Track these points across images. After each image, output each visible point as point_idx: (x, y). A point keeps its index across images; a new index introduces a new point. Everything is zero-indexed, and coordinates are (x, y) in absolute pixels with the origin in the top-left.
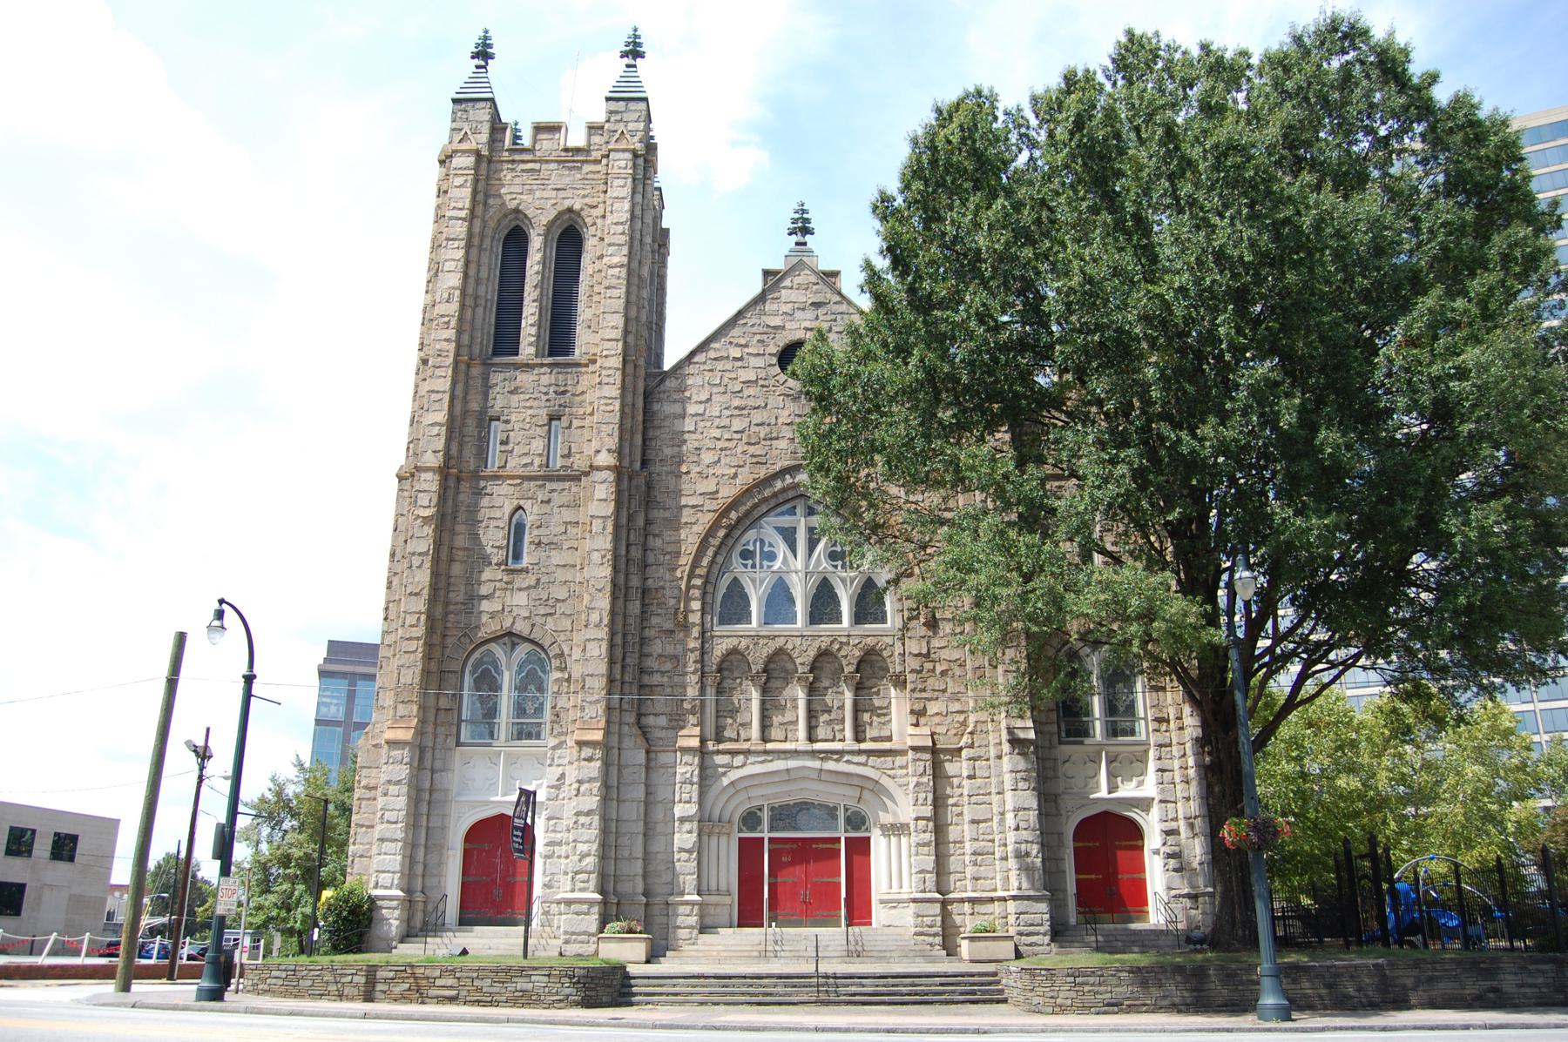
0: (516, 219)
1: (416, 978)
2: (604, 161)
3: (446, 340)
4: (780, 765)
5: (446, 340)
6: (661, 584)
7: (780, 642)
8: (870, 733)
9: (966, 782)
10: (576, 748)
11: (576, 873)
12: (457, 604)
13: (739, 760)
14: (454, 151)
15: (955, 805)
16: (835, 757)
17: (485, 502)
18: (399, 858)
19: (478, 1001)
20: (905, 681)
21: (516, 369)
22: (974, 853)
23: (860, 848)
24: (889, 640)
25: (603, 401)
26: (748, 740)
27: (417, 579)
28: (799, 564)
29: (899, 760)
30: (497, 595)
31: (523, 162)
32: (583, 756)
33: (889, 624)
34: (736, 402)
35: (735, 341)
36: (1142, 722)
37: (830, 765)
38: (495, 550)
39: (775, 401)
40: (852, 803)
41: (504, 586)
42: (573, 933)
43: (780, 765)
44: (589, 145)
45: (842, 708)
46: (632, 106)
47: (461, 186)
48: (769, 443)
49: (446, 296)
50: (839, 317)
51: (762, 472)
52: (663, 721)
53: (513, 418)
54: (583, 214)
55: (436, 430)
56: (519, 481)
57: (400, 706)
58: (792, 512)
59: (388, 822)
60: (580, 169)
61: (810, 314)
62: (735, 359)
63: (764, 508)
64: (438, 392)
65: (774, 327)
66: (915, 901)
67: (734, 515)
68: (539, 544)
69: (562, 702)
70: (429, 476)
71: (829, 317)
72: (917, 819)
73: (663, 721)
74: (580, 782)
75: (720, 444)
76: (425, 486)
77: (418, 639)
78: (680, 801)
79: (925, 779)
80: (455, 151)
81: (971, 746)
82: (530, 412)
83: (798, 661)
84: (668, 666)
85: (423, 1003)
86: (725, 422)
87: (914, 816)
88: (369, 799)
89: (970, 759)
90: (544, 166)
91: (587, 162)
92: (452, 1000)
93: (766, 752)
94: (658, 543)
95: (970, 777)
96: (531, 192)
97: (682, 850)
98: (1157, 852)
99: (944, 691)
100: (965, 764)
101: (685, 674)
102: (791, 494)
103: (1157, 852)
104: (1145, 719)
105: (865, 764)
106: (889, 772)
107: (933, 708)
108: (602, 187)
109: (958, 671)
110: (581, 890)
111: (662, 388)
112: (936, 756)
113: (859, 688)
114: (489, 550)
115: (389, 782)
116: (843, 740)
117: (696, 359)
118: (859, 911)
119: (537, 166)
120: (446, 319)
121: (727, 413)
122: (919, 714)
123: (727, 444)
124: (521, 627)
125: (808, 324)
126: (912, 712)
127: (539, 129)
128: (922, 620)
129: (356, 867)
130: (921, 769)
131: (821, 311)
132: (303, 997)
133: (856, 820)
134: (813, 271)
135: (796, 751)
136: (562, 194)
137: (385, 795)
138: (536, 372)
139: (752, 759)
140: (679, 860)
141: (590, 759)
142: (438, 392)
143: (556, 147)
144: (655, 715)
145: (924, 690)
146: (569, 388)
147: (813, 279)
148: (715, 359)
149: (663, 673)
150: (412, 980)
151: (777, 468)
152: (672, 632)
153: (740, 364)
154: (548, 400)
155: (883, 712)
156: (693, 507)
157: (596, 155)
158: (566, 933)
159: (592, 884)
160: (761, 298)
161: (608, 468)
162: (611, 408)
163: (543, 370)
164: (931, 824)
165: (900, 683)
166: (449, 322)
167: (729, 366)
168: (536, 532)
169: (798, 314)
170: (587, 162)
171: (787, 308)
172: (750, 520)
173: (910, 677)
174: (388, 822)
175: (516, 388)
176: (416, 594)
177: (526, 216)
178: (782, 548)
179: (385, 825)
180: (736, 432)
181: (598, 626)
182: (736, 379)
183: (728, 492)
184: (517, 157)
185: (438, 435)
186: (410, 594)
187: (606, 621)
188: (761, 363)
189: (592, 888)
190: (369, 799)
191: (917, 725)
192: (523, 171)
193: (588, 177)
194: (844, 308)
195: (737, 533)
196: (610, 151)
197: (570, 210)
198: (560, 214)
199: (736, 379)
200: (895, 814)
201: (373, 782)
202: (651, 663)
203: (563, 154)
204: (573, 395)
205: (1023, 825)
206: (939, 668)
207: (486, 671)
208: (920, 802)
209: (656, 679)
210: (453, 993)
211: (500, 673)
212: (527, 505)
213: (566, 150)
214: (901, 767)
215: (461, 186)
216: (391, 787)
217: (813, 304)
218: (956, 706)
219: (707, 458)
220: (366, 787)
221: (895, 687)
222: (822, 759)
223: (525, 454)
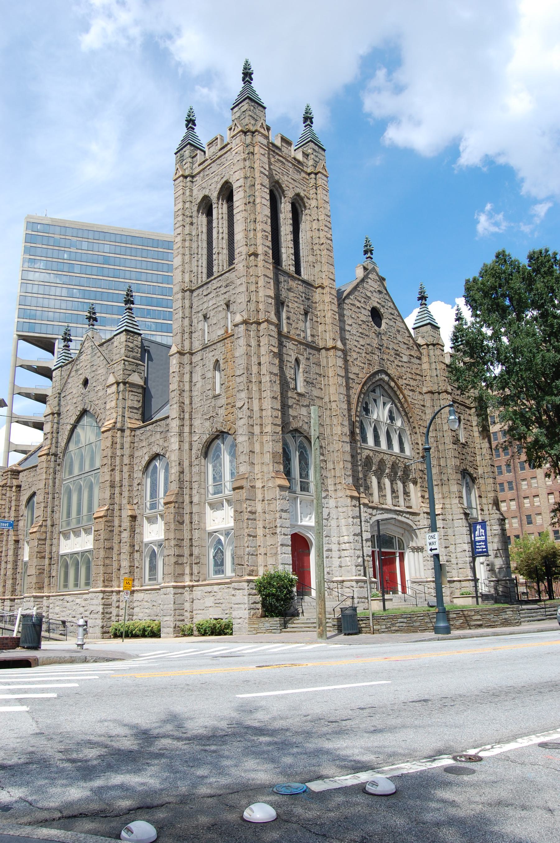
1: (465, 617)
2: (313, 176)
3: (268, 247)
4: (386, 516)
5: (268, 247)
9: (442, 529)
10: (349, 499)
14: (256, 131)
17: (284, 349)
18: (291, 556)
19: (490, 626)
20: (417, 482)
21: (289, 277)
22: (447, 561)
23: (402, 556)
25: (333, 312)
26: (372, 502)
27: (275, 389)
29: (417, 518)
30: (294, 406)
31: (278, 154)
32: (353, 504)
34: (361, 331)
35: (358, 298)
37: (400, 518)
38: (291, 380)
41: (297, 402)
42: (361, 598)
43: (386, 516)
45: (397, 491)
47: (264, 155)
48: (372, 355)
49: (265, 219)
50: (386, 301)
53: (290, 304)
54: (306, 200)
56: (297, 343)
57: (275, 464)
59: (285, 534)
60: (300, 173)
62: (358, 308)
64: (268, 277)
65: (368, 297)
67: (365, 388)
68: (307, 382)
70: (272, 327)
74: (353, 518)
76: (272, 334)
77: (279, 425)
80: (259, 132)
81: (442, 514)
82: (296, 304)
83: (388, 466)
85: (470, 629)
86: (358, 339)
88: (252, 519)
90: (286, 163)
92: (480, 626)
93: (382, 509)
95: (443, 528)
96: (283, 175)
97: (368, 556)
98: (482, 563)
100: (441, 521)
101: (357, 466)
102: (379, 383)
103: (482, 563)
104: (476, 509)
105: (408, 518)
108: (313, 191)
110: (359, 575)
113: (404, 483)
114: (289, 380)
115: (282, 510)
117: (346, 301)
119: (284, 160)
120: (267, 234)
121: (359, 335)
123: (360, 351)
125: (379, 301)
127: (283, 139)
128: (421, 455)
129: (249, 561)
132: (416, 632)
134: (378, 275)
136: (296, 184)
137: (281, 518)
138: (296, 282)
139: (379, 512)
141: (355, 506)
142: (268, 277)
145: (423, 487)
146: (311, 298)
147: (377, 278)
148: (351, 304)
150: (463, 618)
153: (359, 310)
154: (303, 301)
156: (352, 379)
157: (305, 169)
158: (358, 598)
160: (363, 281)
162: (335, 317)
163: (300, 282)
165: (415, 483)
166: (267, 236)
168: (306, 375)
169: (374, 293)
170: (303, 170)
171: (372, 289)
173: (419, 480)
174: (285, 534)
175: (291, 288)
176: (276, 398)
177: (281, 187)
179: (283, 536)
180: (362, 345)
181: (346, 435)
183: (363, 376)
184: (276, 151)
185: (271, 304)
186: (273, 397)
187: (348, 433)
188: (365, 315)
189: (363, 574)
190: (252, 519)
191: (423, 502)
192: (278, 159)
193: (304, 179)
194: (387, 298)
196: (319, 172)
197: (298, 195)
200: (416, 543)
201: (254, 510)
204: (312, 302)
210: (481, 622)
211: (290, 452)
212: (301, 358)
213: (295, 158)
215: (264, 155)
216: (283, 514)
217: (379, 291)
219: (355, 355)
220: (250, 512)
221: (413, 484)
222: (398, 515)
223: (297, 328)
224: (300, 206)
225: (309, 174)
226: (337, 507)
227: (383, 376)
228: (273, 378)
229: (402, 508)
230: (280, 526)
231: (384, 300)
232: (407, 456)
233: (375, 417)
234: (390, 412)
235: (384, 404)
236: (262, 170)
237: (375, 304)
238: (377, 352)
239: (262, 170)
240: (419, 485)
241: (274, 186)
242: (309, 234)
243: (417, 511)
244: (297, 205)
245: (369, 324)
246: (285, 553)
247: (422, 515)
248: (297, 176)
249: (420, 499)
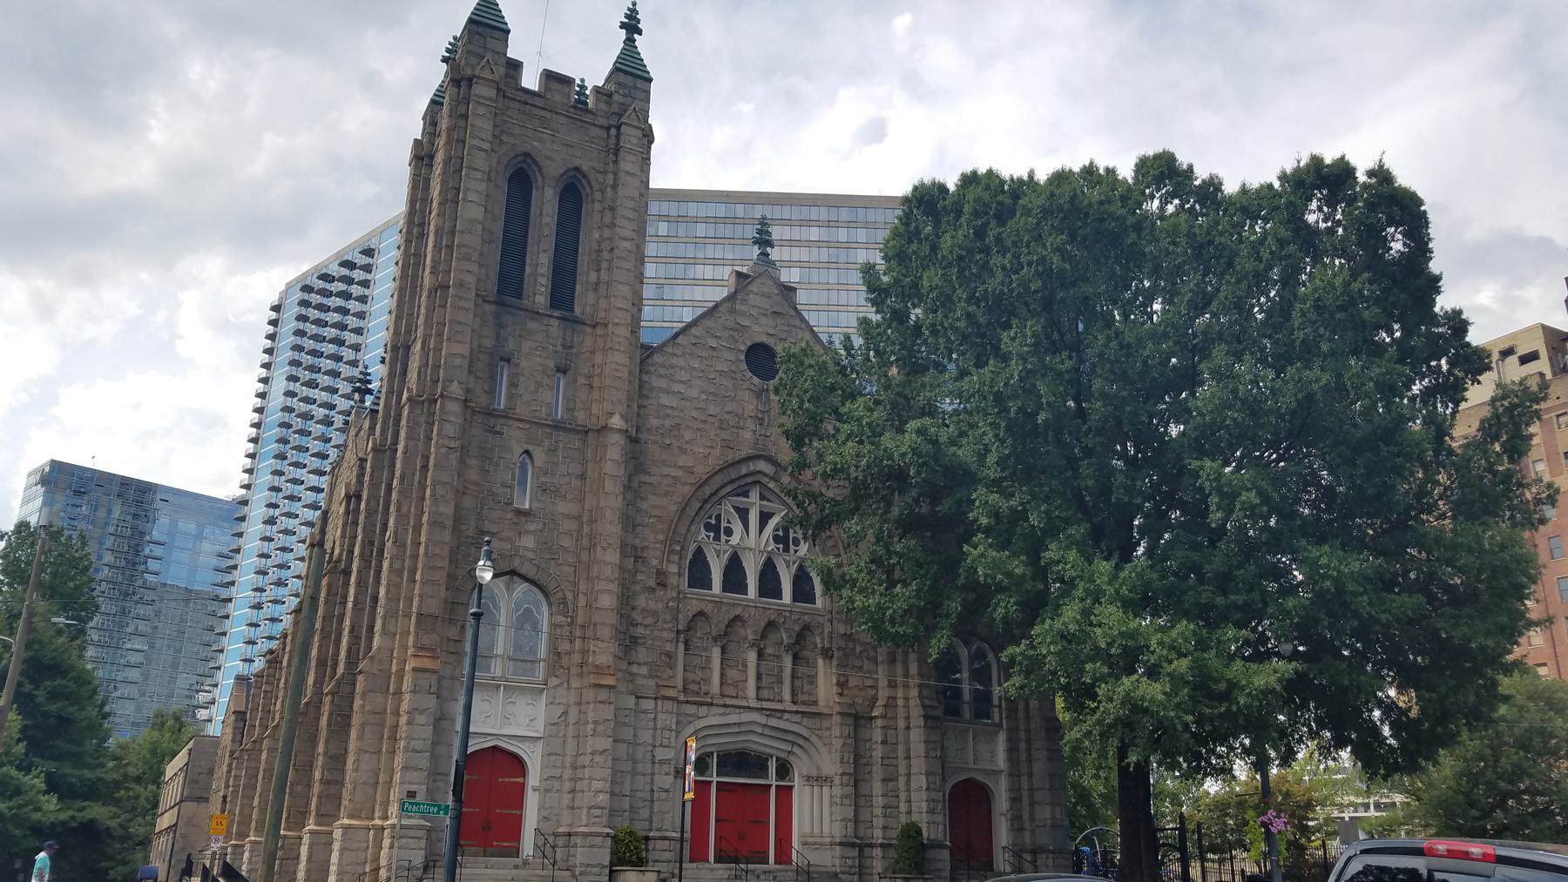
0: (524, 162)
4: (734, 718)
6: (646, 544)
7: (738, 611)
8: (801, 698)
11: (590, 808)
12: (468, 537)
13: (703, 710)
14: (474, 76)
15: (865, 765)
16: (778, 715)
20: (832, 657)
23: (785, 793)
24: (820, 619)
28: (752, 541)
33: (819, 603)
36: (996, 710)
39: (746, 395)
40: (783, 755)
43: (734, 718)
44: (597, 110)
46: (640, 83)
51: (730, 457)
52: (644, 670)
53: (523, 363)
54: (592, 176)
55: (458, 362)
58: (746, 494)
61: (771, 322)
63: (729, 489)
64: (460, 323)
66: (841, 844)
69: (564, 646)
71: (786, 328)
72: (843, 774)
73: (644, 670)
75: (696, 425)
78: (661, 745)
79: (849, 741)
80: (479, 77)
84: (649, 621)
86: (702, 405)
87: (840, 771)
89: (884, 727)
91: (594, 125)
93: (725, 706)
94: (644, 505)
96: (540, 140)
99: (861, 668)
102: (750, 479)
106: (817, 732)
107: (852, 683)
109: (872, 653)
111: (650, 361)
112: (857, 719)
116: (780, 701)
118: (783, 855)
119: (548, 115)
122: (842, 685)
124: (526, 569)
126: (839, 684)
130: (847, 733)
131: (779, 321)
133: (784, 770)
135: (749, 708)
139: (714, 710)
140: (658, 800)
143: (565, 101)
144: (638, 664)
149: (646, 626)
151: (743, 454)
152: (654, 589)
155: (812, 680)
156: (673, 477)
159: (604, 820)
161: (620, 431)
162: (619, 374)
164: (852, 779)
165: (827, 654)
167: (705, 354)
169: (763, 320)
172: (715, 497)
177: (535, 161)
178: (737, 528)
182: (711, 366)
183: (702, 471)
188: (731, 358)
191: (840, 694)
195: (708, 506)
196: (622, 123)
197: (577, 169)
198: (568, 170)
199: (711, 366)
202: (636, 616)
203: (572, 110)
205: (932, 786)
206: (858, 649)
207: (528, 610)
208: (845, 760)
209: (640, 630)
214: (827, 729)
218: (870, 683)
224: (584, 188)
225: (608, 129)
226: (579, 704)
227: (762, 466)
228: (440, 491)
229: (788, 706)
230: (405, 739)
231: (786, 328)
232: (817, 610)
233: (735, 539)
234: (785, 527)
235: (764, 518)
236: (477, 142)
237: (763, 339)
238: (750, 424)
239: (477, 142)
240: (835, 662)
241: (524, 162)
242: (596, 235)
243: (825, 711)
244: (579, 186)
245: (739, 376)
246: (410, 783)
247: (834, 717)
248: (574, 138)
249: (835, 689)
